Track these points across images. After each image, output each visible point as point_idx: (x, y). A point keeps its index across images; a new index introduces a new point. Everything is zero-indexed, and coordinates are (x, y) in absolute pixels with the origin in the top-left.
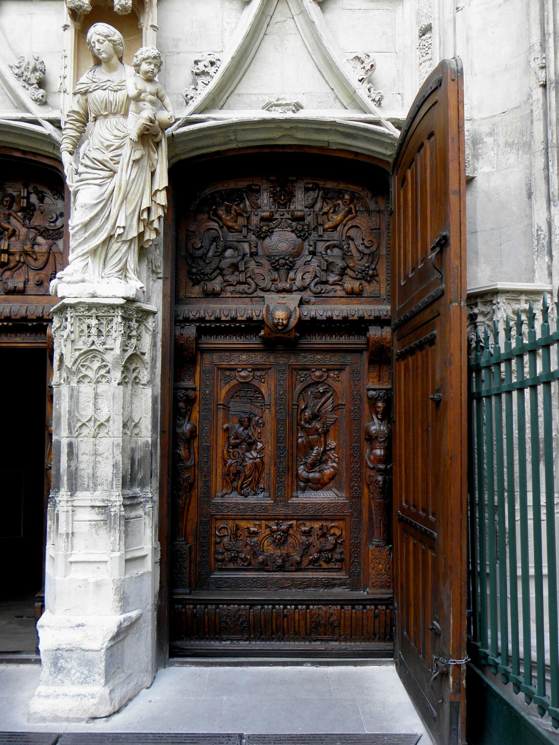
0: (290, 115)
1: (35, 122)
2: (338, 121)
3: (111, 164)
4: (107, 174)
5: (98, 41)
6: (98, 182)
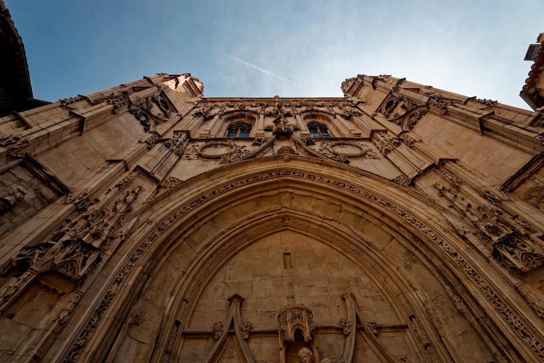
5: (305, 356)
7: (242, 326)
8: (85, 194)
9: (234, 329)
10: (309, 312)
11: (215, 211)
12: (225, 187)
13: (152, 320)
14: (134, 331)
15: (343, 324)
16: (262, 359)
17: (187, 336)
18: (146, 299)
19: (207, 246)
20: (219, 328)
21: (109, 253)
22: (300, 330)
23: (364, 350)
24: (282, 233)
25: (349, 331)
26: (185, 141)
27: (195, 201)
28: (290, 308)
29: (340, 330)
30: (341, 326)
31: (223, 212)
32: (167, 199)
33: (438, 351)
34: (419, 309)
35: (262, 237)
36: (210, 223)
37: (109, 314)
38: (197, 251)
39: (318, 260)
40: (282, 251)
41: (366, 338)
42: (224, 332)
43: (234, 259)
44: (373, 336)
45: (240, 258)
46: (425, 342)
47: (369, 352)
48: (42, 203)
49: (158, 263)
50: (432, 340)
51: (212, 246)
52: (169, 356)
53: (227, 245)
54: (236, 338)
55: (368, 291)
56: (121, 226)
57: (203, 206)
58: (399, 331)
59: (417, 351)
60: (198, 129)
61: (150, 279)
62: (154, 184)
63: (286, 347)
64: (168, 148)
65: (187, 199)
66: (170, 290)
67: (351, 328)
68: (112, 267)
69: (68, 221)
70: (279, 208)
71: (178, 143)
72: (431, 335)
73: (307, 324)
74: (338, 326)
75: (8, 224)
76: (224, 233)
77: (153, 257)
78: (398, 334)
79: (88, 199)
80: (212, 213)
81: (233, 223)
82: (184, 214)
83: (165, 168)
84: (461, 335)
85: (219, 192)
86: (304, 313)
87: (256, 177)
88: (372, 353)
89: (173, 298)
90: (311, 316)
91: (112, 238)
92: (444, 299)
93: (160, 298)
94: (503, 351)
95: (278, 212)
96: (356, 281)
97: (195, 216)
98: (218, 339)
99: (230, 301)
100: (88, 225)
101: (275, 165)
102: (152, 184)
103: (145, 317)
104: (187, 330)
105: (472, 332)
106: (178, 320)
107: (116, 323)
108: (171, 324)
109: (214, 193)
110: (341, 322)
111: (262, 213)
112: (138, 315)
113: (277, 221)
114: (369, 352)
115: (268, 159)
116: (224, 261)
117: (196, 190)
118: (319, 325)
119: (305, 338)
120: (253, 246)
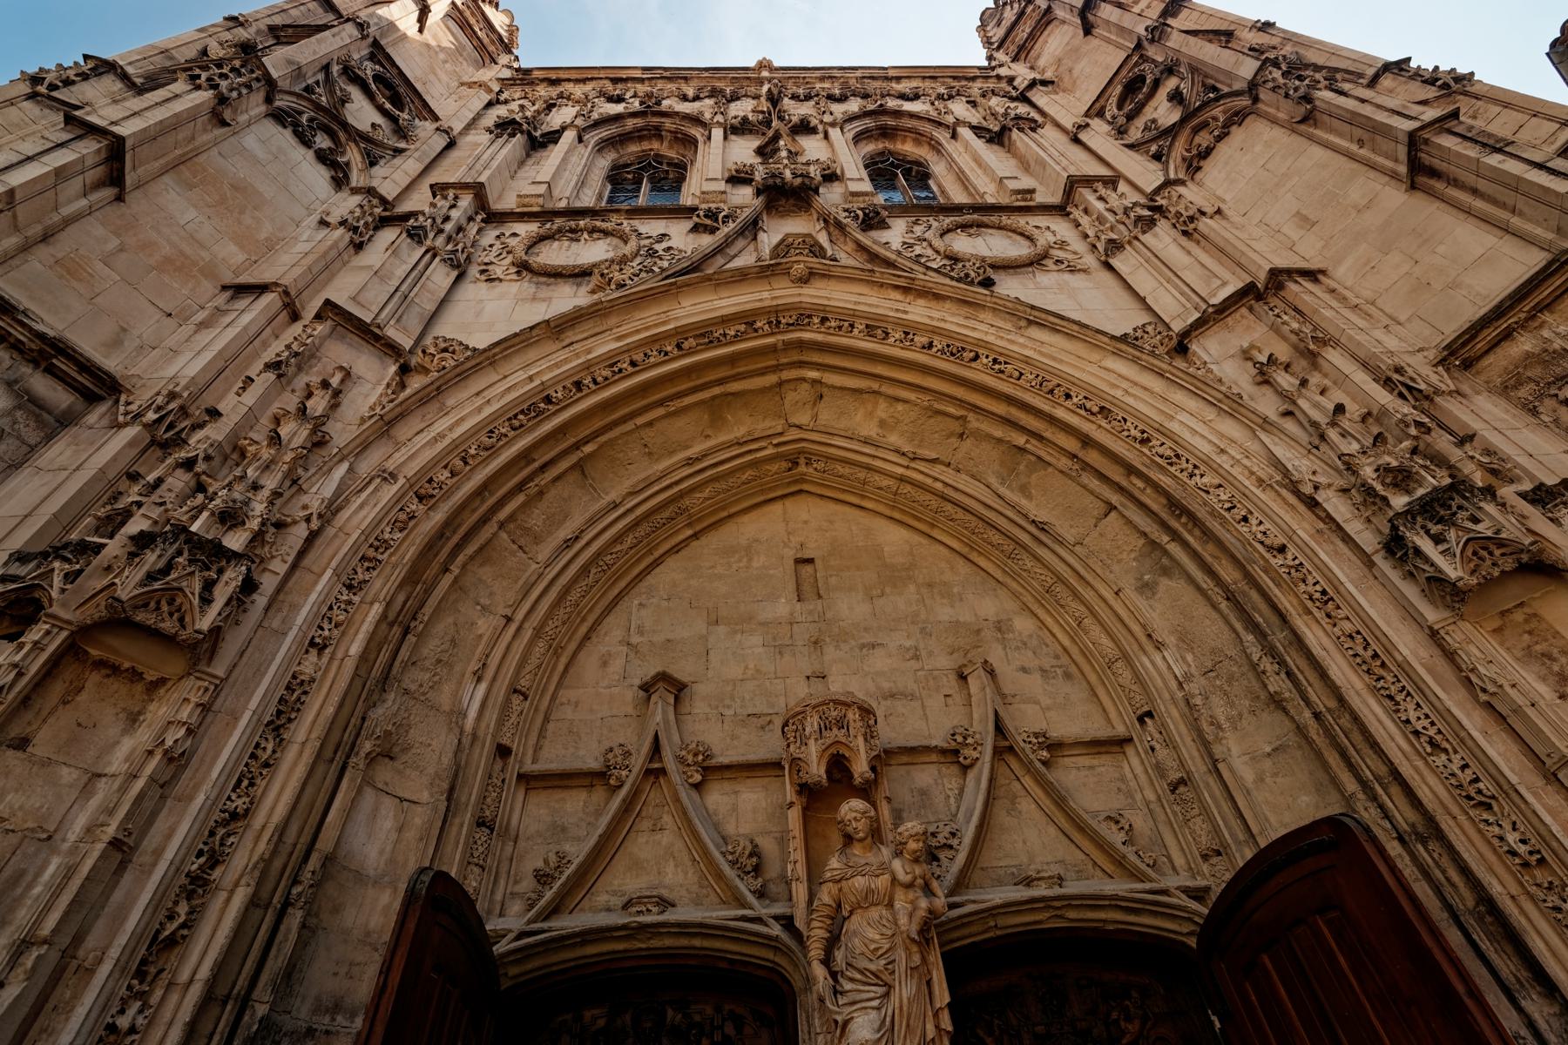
0: (1057, 891)
1: (758, 920)
2: (1121, 893)
3: (886, 977)
4: (881, 990)
5: (855, 819)
6: (875, 1003)
7: (684, 753)
8: (172, 396)
9: (661, 760)
10: (866, 711)
11: (586, 441)
12: (612, 366)
13: (430, 745)
14: (384, 773)
15: (960, 739)
16: (742, 831)
17: (528, 781)
18: (406, 692)
19: (568, 543)
20: (619, 759)
21: (279, 567)
22: (843, 756)
23: (1013, 799)
24: (788, 502)
25: (975, 754)
26: (470, 219)
27: (522, 412)
28: (814, 702)
29: (953, 755)
30: (954, 744)
31: (611, 442)
32: (433, 406)
33: (1206, 795)
34: (1167, 696)
35: (730, 516)
36: (571, 478)
38: (542, 557)
39: (894, 576)
40: (790, 554)
41: (1019, 772)
42: (635, 770)
43: (650, 580)
44: (1038, 765)
45: (669, 574)
46: (1175, 775)
47: (1026, 805)
48: (40, 423)
49: (428, 592)
50: (1193, 769)
51: (582, 542)
52: (488, 831)
53: (629, 540)
54: (669, 782)
55: (1030, 654)
57: (547, 427)
58: (1107, 753)
59: (1151, 796)
60: (512, 178)
61: (411, 639)
62: (390, 361)
63: (805, 800)
64: (420, 243)
65: (495, 406)
67: (979, 748)
68: (295, 608)
69: (134, 477)
70: (779, 429)
71: (448, 227)
72: (1192, 758)
73: (860, 740)
74: (945, 745)
76: (616, 506)
77: (412, 577)
78: (1105, 759)
79: (182, 408)
80: (577, 446)
81: (642, 476)
83: (415, 310)
84: (1269, 755)
85: (595, 381)
86: (853, 715)
87: (705, 333)
88: (1033, 806)
89: (483, 687)
90: (872, 722)
91: (280, 525)
92: (1235, 669)
93: (447, 689)
94: (1372, 789)
95: (775, 442)
96: (999, 630)
97: (525, 456)
98: (620, 787)
99: (646, 691)
101: (766, 295)
102: (380, 358)
103: (410, 736)
104: (529, 767)
105: (1300, 747)
106: (504, 742)
107: (328, 754)
108: (485, 754)
109: (578, 385)
110: (953, 735)
112: (388, 734)
113: (774, 467)
114: (1026, 805)
115: (742, 276)
116: (622, 584)
117: (521, 375)
118: (895, 744)
119: (856, 776)
120: (704, 540)
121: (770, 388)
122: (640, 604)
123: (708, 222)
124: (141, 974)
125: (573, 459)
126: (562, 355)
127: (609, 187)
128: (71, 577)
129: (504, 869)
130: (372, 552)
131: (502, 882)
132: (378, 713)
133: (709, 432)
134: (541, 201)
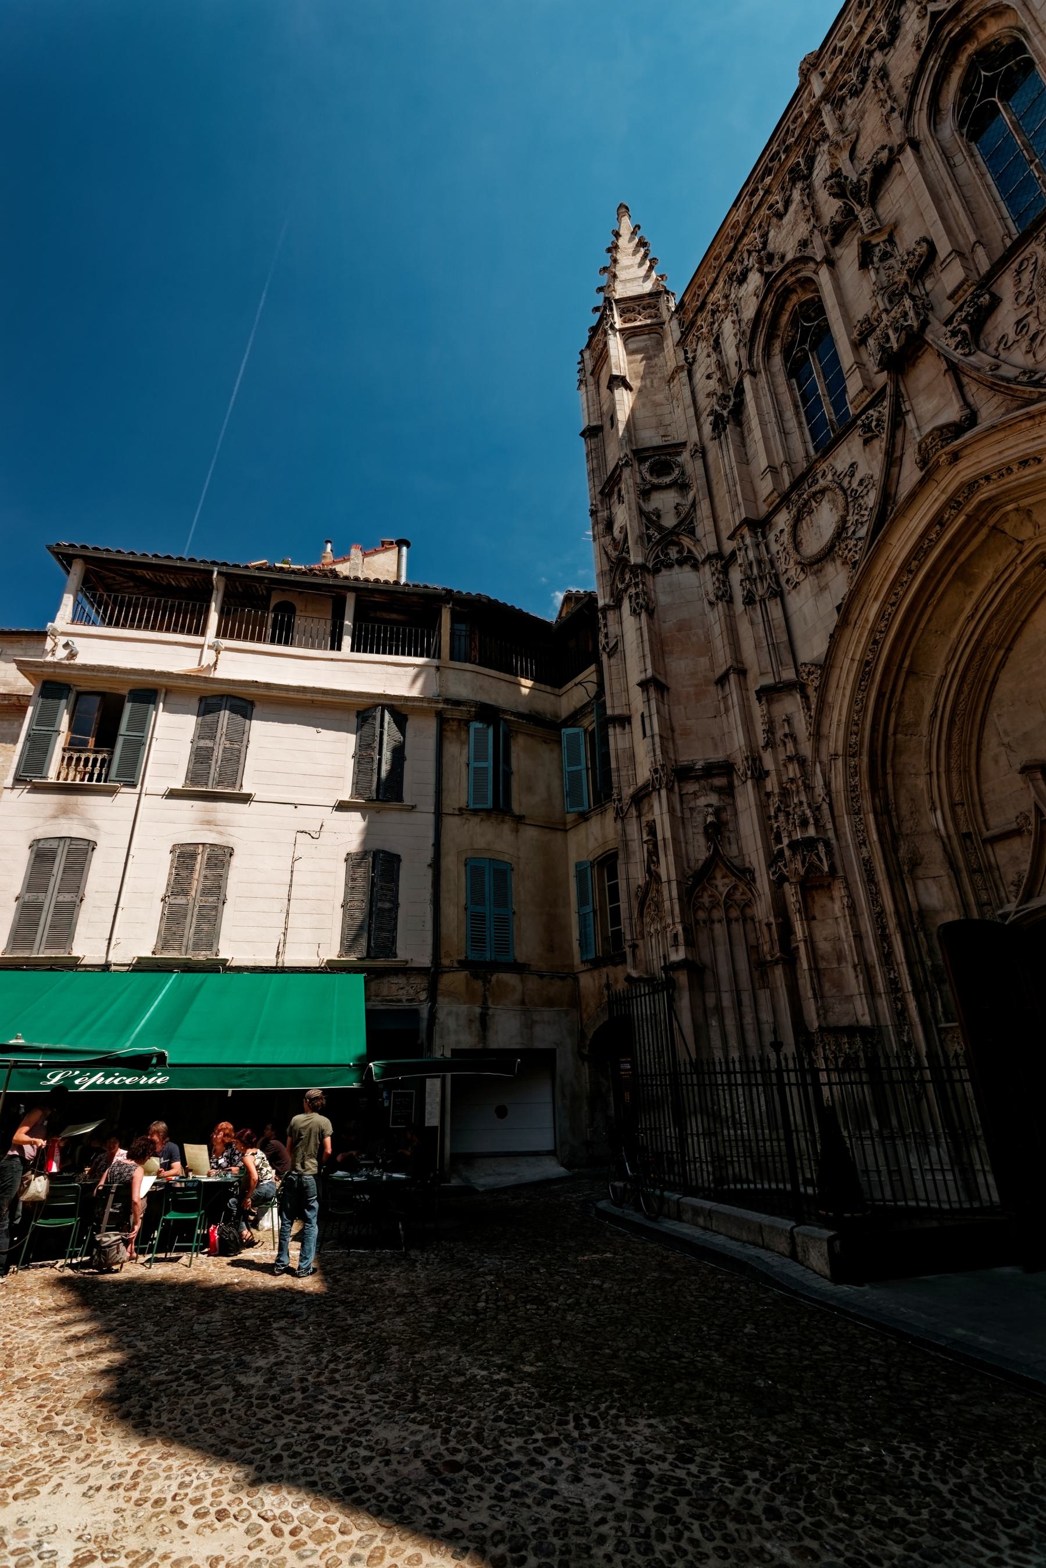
12: (883, 617)
14: (920, 872)
18: (907, 835)
19: (933, 715)
21: (829, 826)
26: (757, 545)
27: (862, 680)
31: (916, 648)
35: (1024, 622)
37: (881, 876)
38: (925, 732)
43: (997, 695)
45: (1005, 686)
49: (885, 788)
51: (941, 708)
53: (966, 689)
56: (813, 788)
60: (748, 464)
62: (794, 692)
64: (755, 602)
66: (928, 806)
68: (845, 834)
70: (1016, 552)
75: (732, 836)
76: (945, 677)
77: (874, 789)
80: (900, 667)
81: (947, 648)
82: (864, 708)
83: (782, 646)
85: (881, 632)
87: (919, 552)
91: (818, 808)
95: (1019, 561)
97: (880, 695)
100: (788, 814)
101: (936, 493)
102: (791, 695)
104: (987, 834)
109: (875, 642)
111: (989, 588)
112: (910, 859)
115: (913, 496)
116: (980, 710)
117: (847, 662)
121: (988, 536)
122: (999, 715)
123: (870, 434)
124: (887, 964)
125: (903, 675)
126: (856, 634)
127: (794, 381)
128: (785, 866)
129: (999, 882)
130: (852, 790)
131: (1001, 889)
132: (902, 852)
133: (969, 590)
134: (775, 494)
